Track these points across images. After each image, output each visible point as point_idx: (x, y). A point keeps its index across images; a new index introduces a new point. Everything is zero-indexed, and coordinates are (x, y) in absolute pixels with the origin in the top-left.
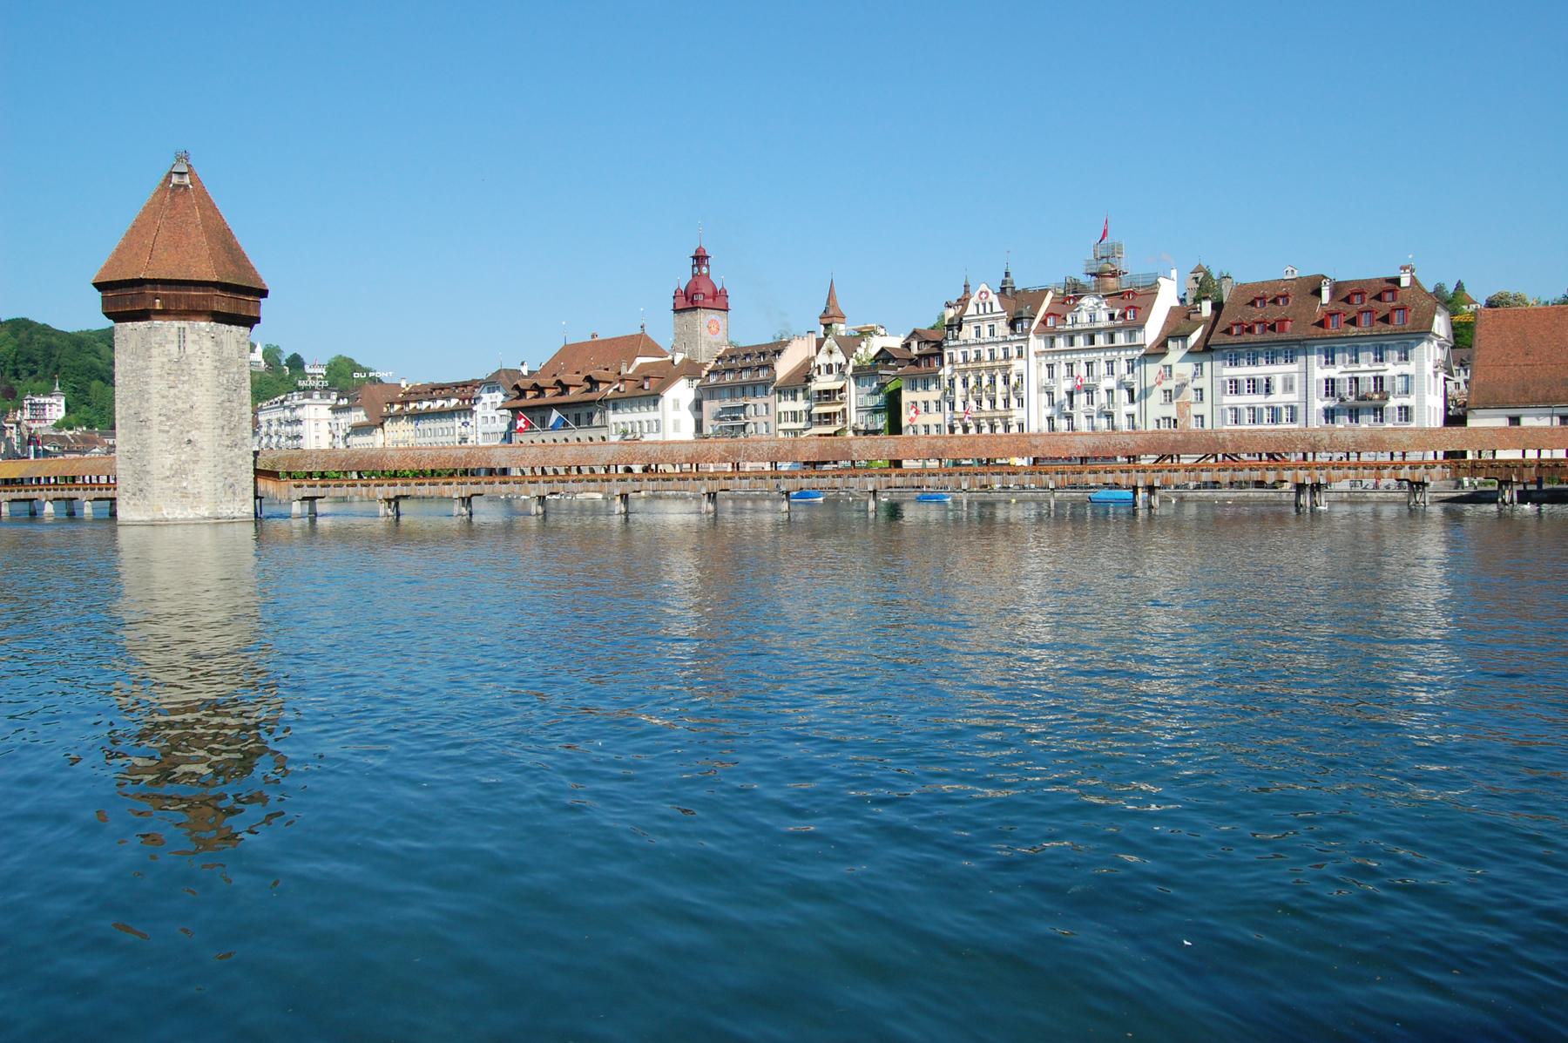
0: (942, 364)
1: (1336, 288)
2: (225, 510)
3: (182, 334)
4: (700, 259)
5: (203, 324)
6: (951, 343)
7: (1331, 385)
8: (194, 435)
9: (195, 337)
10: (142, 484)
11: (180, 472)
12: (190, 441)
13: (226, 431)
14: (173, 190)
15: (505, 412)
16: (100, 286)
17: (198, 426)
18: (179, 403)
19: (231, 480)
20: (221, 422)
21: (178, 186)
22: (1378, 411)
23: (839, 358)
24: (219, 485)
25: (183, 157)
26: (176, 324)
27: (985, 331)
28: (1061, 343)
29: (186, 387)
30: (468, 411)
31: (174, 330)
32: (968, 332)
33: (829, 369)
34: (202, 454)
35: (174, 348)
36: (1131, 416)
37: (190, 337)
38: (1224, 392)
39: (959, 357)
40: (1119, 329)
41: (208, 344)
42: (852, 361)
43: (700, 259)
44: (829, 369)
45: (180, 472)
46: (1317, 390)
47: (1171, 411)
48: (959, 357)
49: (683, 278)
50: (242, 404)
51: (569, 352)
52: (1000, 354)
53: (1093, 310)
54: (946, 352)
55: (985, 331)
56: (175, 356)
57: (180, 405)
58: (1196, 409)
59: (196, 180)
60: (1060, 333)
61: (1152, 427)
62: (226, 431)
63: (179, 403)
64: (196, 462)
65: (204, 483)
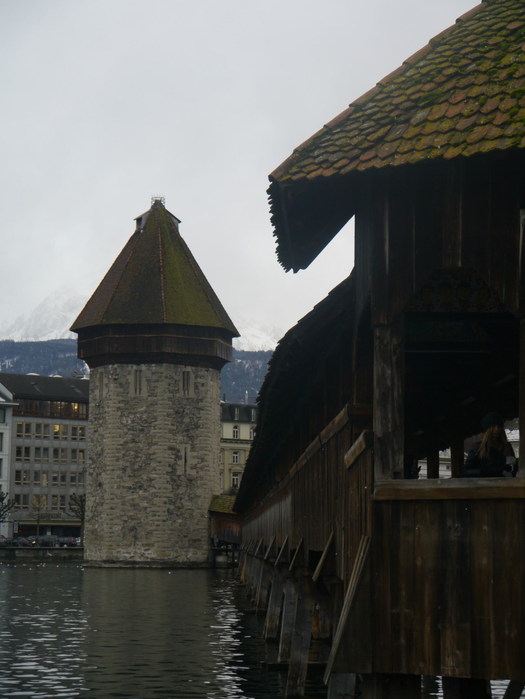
2: (125, 554)
5: (110, 366)
8: (104, 477)
12: (100, 485)
13: (129, 471)
19: (131, 524)
20: (121, 463)
24: (117, 528)
26: (100, 370)
29: (101, 430)
31: (98, 376)
34: (106, 496)
37: (105, 381)
41: (112, 385)
45: (96, 515)
50: (150, 444)
57: (99, 449)
62: (129, 471)
64: (102, 504)
65: (105, 525)
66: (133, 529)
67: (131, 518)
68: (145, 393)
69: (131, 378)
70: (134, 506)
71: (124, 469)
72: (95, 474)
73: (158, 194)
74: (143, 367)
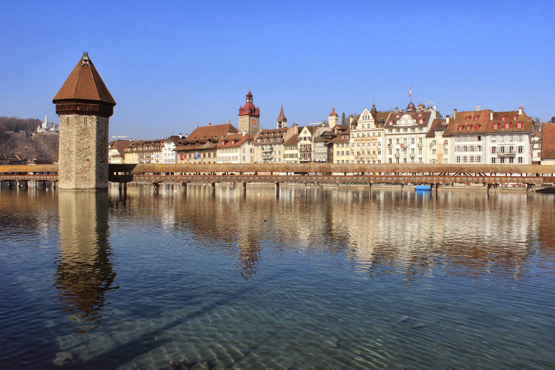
0: (349, 137)
1: (495, 115)
3: (85, 119)
4: (250, 96)
5: (94, 116)
6: (353, 130)
7: (494, 149)
8: (89, 157)
9: (91, 121)
10: (69, 175)
11: (84, 170)
12: (88, 160)
14: (83, 66)
15: (174, 152)
16: (54, 102)
17: (91, 154)
18: (84, 145)
19: (101, 174)
21: (84, 65)
22: (511, 158)
23: (309, 134)
25: (86, 54)
27: (366, 127)
28: (394, 131)
29: (87, 140)
30: (160, 151)
31: (83, 118)
32: (359, 127)
33: (305, 139)
35: (83, 125)
36: (421, 159)
38: (456, 150)
39: (355, 135)
40: (416, 126)
42: (313, 136)
43: (250, 96)
44: (305, 139)
46: (489, 150)
47: (436, 157)
48: (355, 135)
49: (243, 102)
51: (199, 130)
52: (371, 134)
53: (407, 120)
54: (351, 133)
55: (366, 127)
56: (83, 128)
57: (85, 146)
58: (445, 156)
59: (90, 63)
60: (395, 127)
61: (428, 162)
63: (84, 145)
64: (89, 167)
66: (101, 177)
67: (101, 172)
68: (104, 128)
69: (101, 121)
70: (102, 168)
71: (99, 155)
72: (82, 156)
73: (86, 51)
74: (104, 118)
